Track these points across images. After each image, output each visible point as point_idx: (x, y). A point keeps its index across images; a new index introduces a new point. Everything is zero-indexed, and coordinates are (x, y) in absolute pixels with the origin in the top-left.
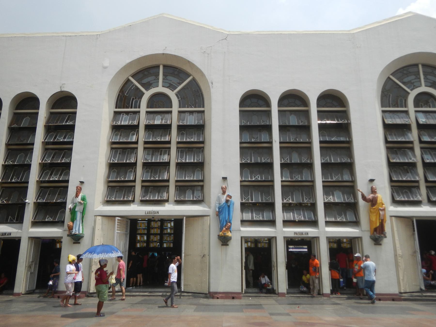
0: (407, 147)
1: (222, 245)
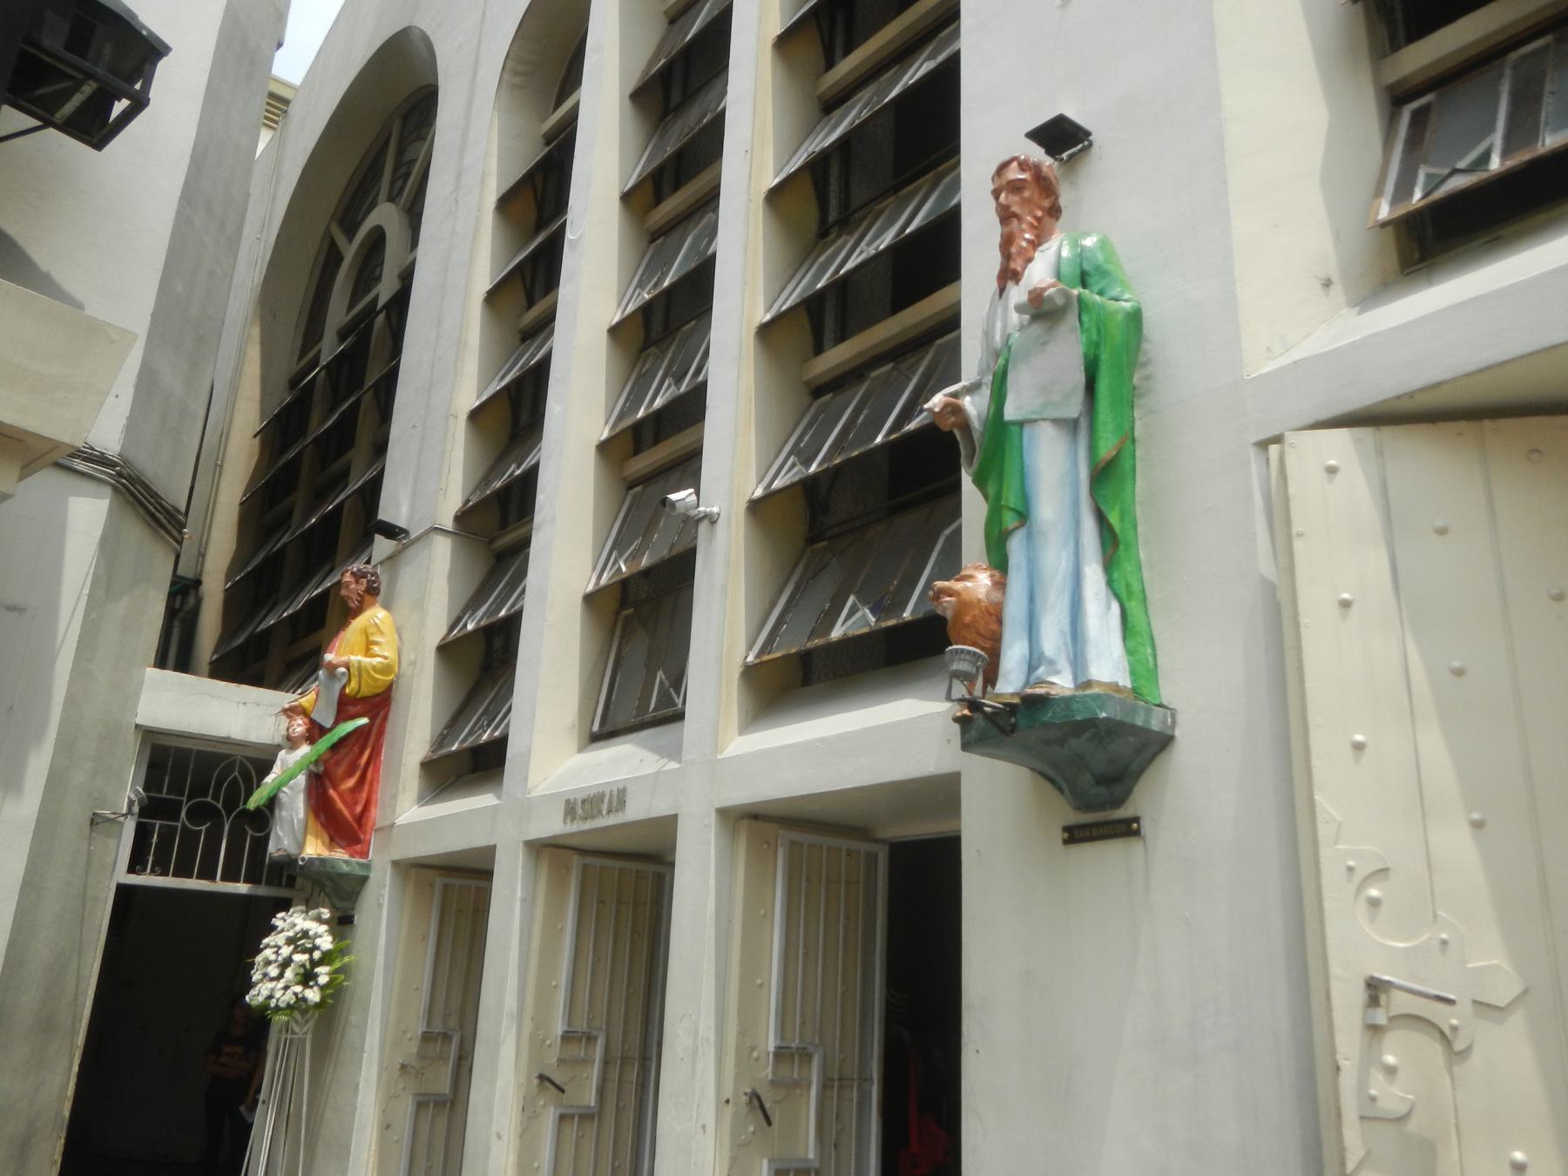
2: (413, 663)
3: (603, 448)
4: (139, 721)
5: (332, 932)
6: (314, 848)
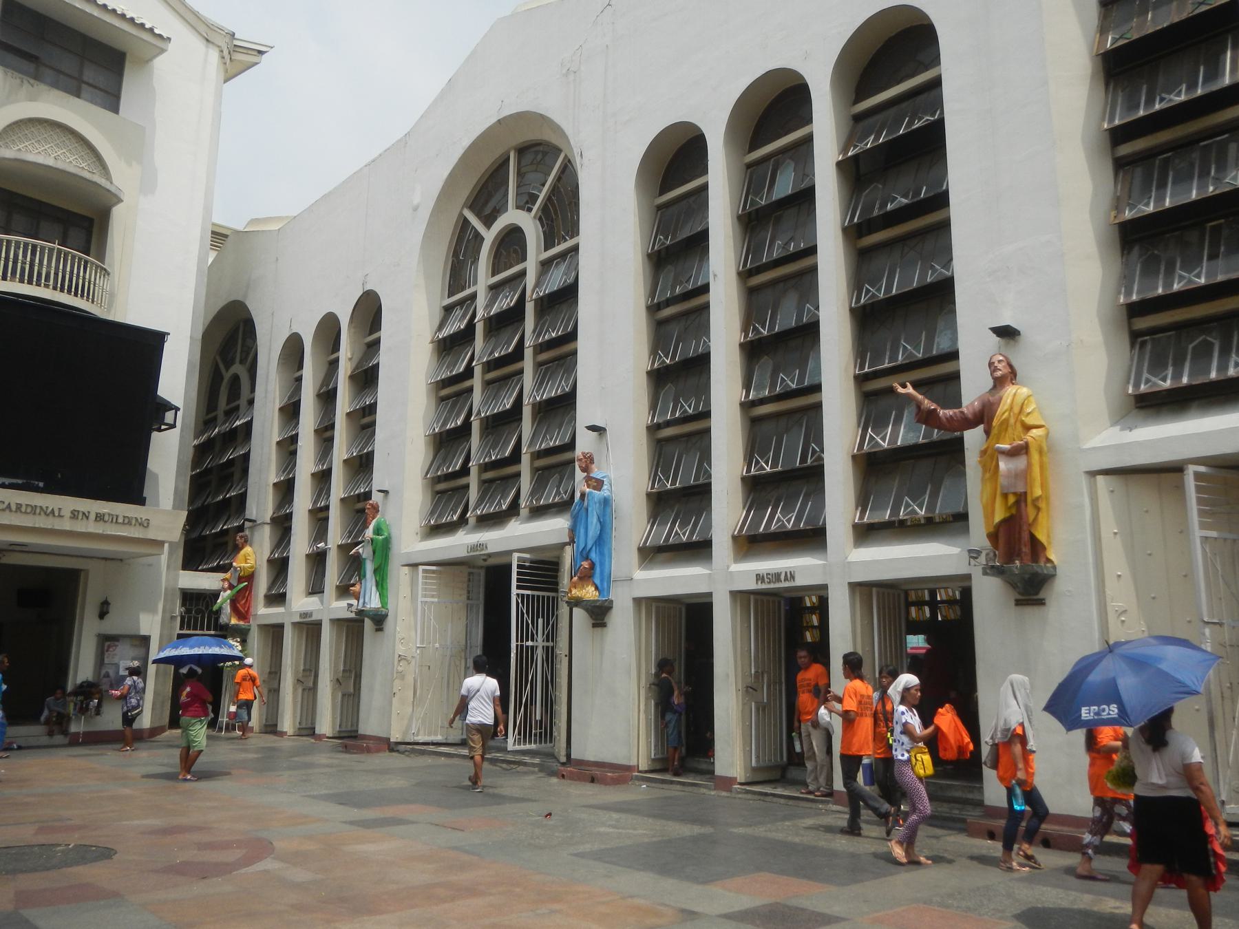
1: (594, 626)
2: (260, 565)
3: (310, 511)
4: (180, 586)
5: (240, 644)
6: (234, 621)
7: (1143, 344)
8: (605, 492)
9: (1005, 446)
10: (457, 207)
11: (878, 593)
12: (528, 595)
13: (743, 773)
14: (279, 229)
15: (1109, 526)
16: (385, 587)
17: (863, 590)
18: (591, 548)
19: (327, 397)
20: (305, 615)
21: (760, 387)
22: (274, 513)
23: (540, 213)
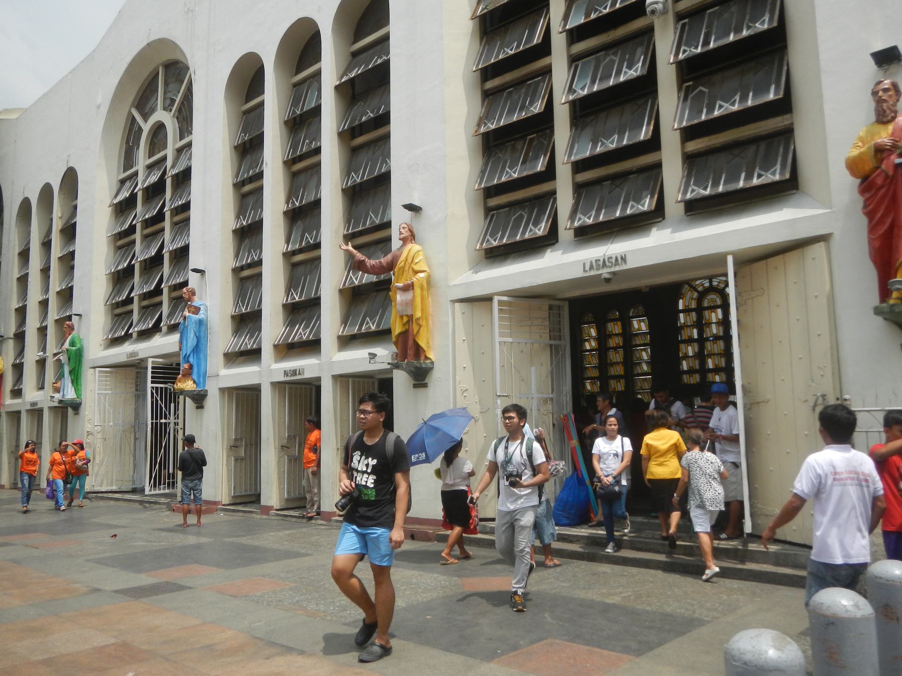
0: (536, 71)
3: (38, 329)
7: (493, 215)
8: (201, 315)
9: (400, 285)
10: (127, 106)
11: (354, 382)
12: (161, 388)
13: (278, 503)
14: (17, 119)
15: (461, 336)
16: (79, 383)
17: (341, 379)
18: (190, 355)
19: (47, 245)
20: (34, 404)
21: (294, 243)
22: (16, 331)
23: (177, 114)
